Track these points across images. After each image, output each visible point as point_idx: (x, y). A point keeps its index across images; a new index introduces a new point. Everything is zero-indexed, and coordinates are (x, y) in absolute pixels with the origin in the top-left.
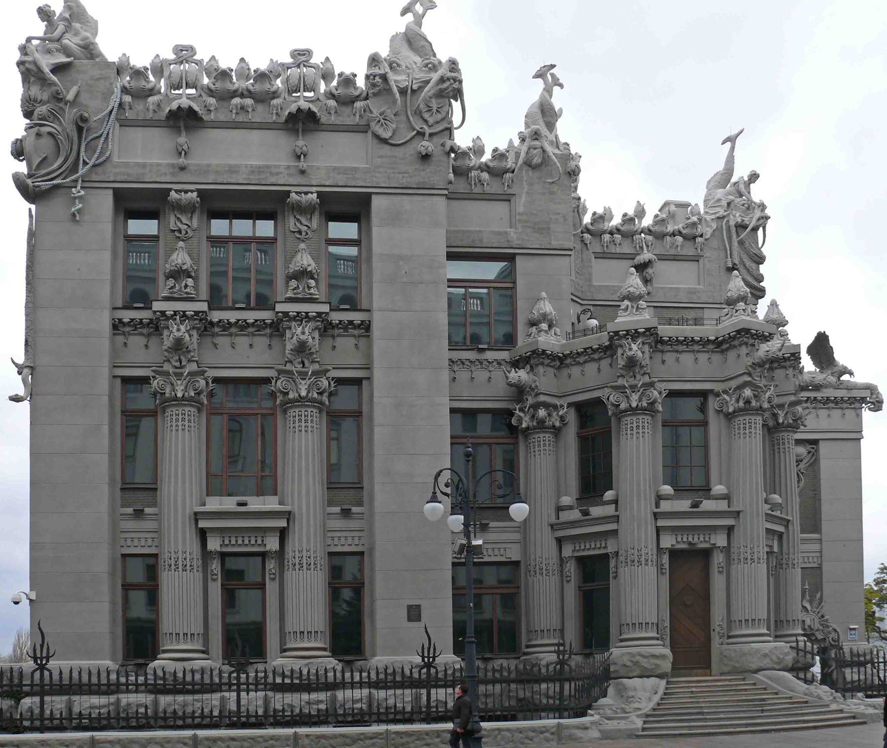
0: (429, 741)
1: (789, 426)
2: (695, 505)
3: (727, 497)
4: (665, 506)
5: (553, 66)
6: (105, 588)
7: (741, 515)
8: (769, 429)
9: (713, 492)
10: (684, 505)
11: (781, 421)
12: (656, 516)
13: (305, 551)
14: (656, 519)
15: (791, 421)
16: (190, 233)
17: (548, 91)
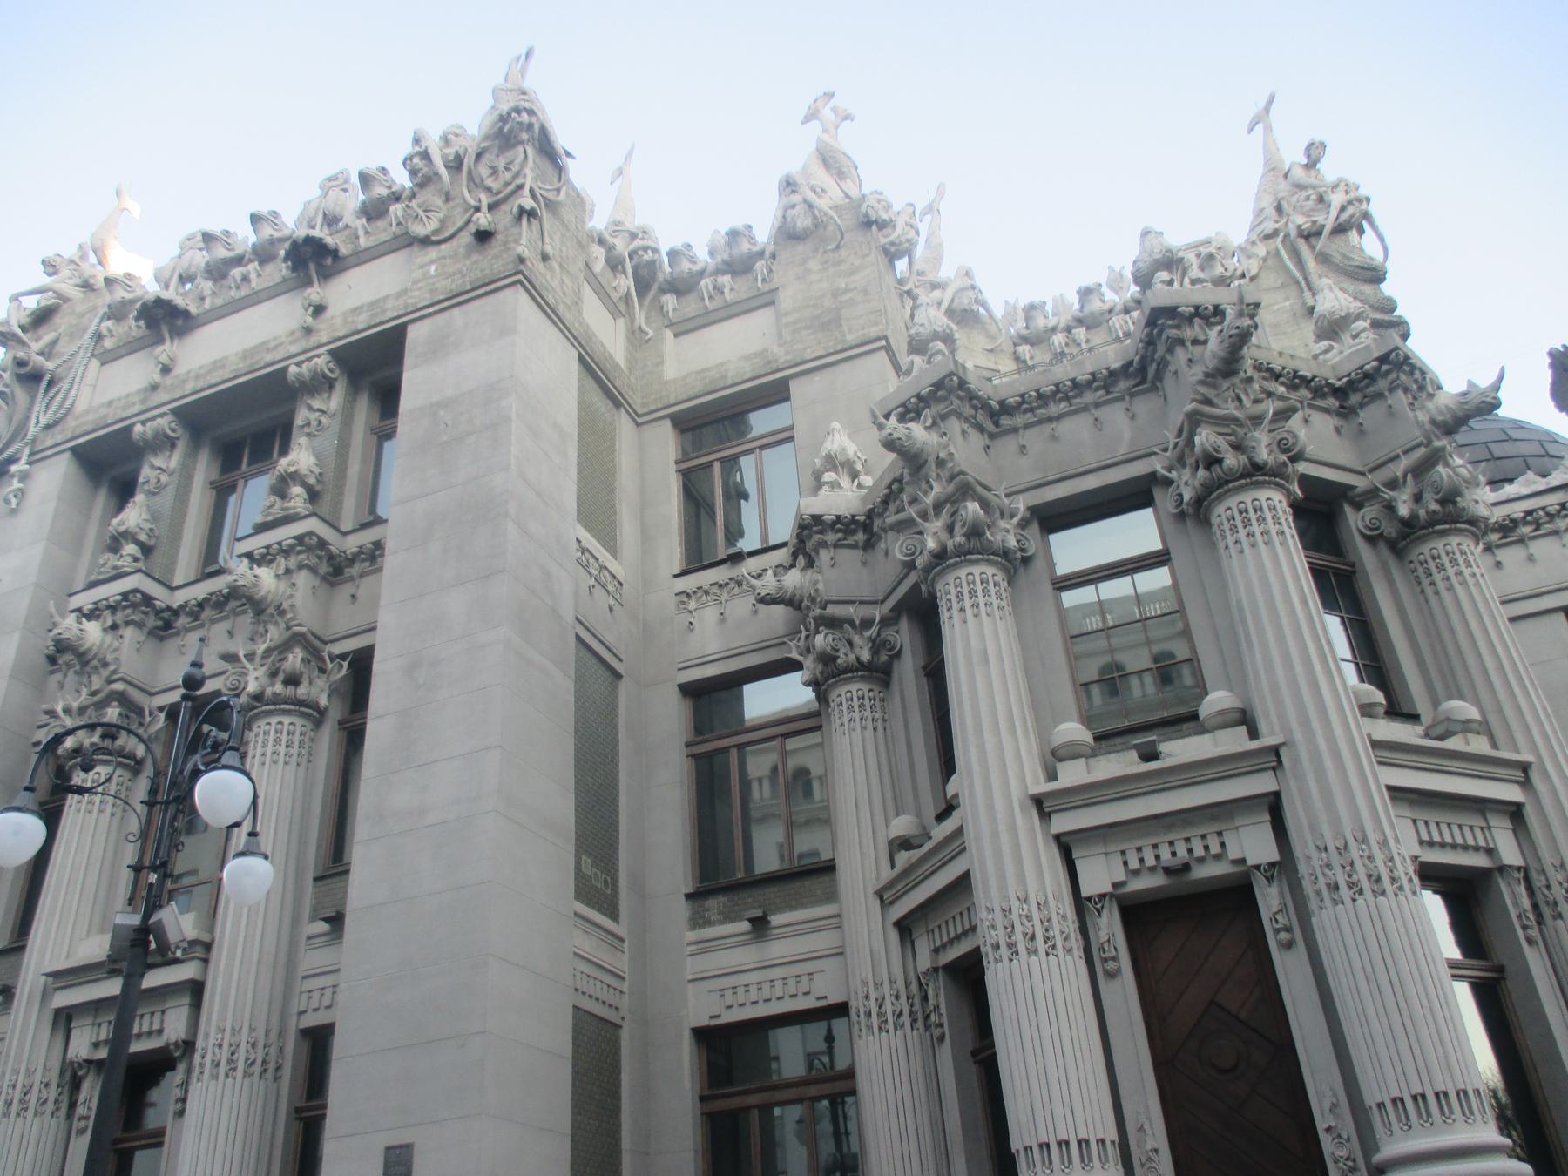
2: (1149, 755)
4: (1072, 774)
7: (1283, 752)
10: (1120, 763)
11: (1404, 511)
12: (1042, 805)
13: (245, 1030)
14: (1045, 816)
15: (1434, 506)
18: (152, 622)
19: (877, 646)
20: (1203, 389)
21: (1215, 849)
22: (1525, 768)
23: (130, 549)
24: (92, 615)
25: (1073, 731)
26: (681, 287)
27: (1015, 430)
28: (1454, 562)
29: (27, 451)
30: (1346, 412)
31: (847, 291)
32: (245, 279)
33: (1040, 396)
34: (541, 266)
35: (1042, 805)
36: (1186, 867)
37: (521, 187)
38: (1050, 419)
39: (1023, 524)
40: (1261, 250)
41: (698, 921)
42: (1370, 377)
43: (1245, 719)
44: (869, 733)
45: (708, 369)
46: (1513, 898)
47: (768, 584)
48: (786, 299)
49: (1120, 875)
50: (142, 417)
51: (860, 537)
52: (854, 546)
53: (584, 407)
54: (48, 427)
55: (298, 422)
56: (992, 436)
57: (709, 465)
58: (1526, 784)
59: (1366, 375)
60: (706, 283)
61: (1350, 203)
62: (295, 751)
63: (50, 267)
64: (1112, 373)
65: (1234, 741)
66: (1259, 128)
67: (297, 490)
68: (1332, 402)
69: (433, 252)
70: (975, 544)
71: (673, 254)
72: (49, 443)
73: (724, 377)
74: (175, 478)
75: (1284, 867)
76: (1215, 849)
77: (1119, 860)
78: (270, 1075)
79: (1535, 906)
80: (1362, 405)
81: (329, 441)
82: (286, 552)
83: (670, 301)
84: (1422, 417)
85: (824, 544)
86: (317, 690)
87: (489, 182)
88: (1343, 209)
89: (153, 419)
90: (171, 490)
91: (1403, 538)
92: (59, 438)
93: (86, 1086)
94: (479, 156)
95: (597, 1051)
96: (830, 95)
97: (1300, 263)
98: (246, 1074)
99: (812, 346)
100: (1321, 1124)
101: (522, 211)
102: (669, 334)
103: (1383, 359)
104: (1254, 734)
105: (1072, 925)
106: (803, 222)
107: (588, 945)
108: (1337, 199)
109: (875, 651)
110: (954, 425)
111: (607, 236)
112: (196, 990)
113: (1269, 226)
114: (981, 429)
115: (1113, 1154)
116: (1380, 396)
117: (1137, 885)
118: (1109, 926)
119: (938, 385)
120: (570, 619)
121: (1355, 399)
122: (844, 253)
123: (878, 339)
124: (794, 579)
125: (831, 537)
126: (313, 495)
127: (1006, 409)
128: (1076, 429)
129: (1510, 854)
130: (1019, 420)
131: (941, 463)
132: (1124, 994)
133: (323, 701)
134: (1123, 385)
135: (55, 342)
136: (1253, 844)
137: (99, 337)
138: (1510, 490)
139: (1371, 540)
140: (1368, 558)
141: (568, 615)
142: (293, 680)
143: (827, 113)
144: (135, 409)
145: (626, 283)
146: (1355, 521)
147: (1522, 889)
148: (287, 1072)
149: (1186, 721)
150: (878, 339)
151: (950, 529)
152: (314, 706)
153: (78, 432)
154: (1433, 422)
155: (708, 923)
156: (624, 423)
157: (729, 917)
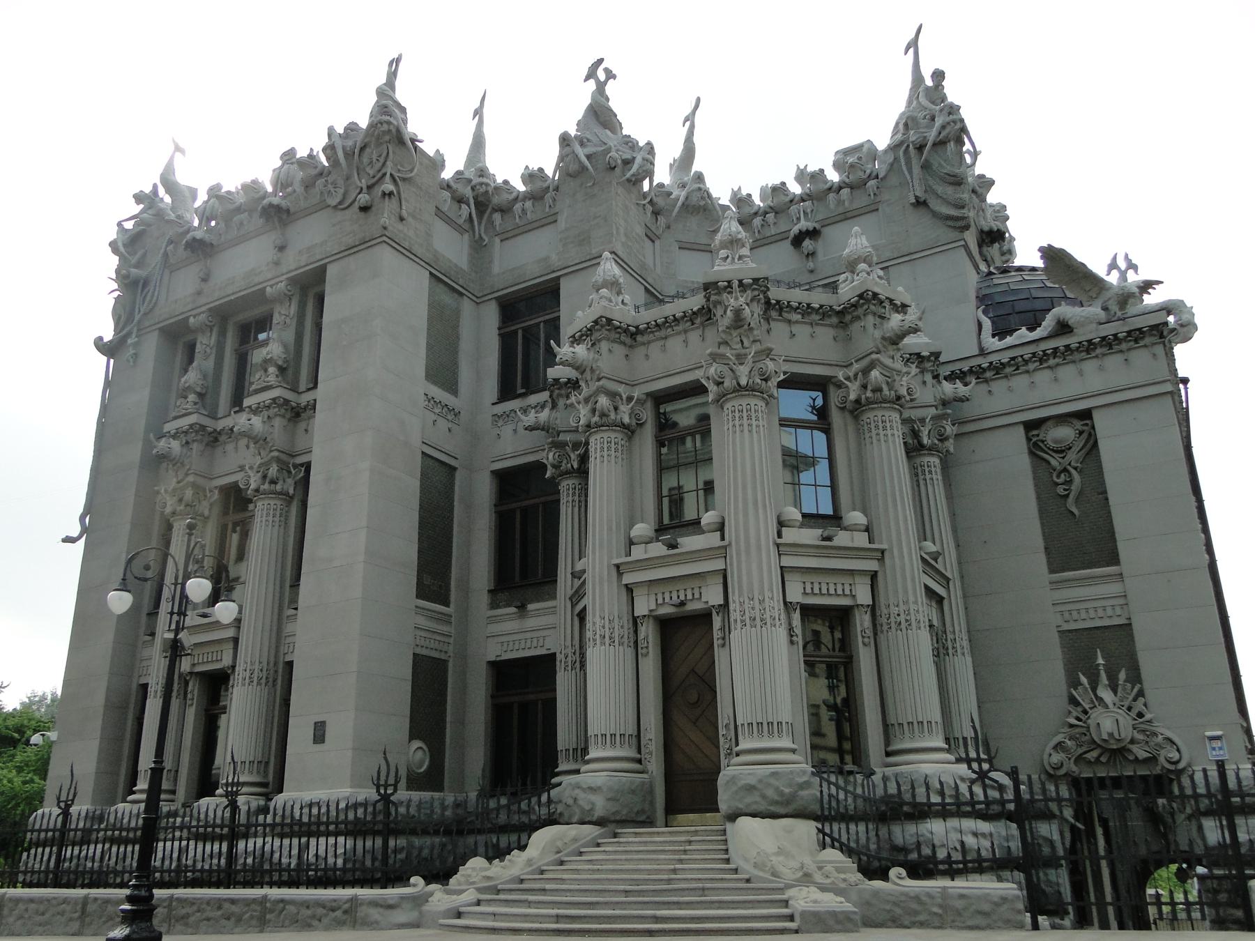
0: (211, 914)
1: (869, 402)
2: (672, 546)
4: (638, 553)
6: (98, 723)
8: (851, 412)
9: (703, 522)
10: (658, 549)
14: (620, 574)
15: (869, 394)
18: (206, 439)
20: (724, 336)
21: (697, 596)
22: (883, 552)
24: (174, 437)
25: (642, 529)
27: (644, 344)
28: (877, 427)
29: (135, 330)
30: (843, 325)
31: (595, 218)
32: (241, 224)
33: (657, 325)
34: (400, 226)
36: (682, 604)
37: (385, 174)
41: (494, 605)
42: (855, 306)
43: (721, 527)
44: (576, 509)
46: (862, 621)
47: (530, 419)
49: (653, 607)
50: (193, 313)
54: (145, 314)
55: (275, 321)
57: (515, 332)
58: (881, 560)
59: (853, 305)
60: (518, 206)
62: (277, 519)
63: (139, 198)
64: (694, 313)
65: (713, 540)
66: (911, 51)
67: (272, 370)
68: (835, 320)
69: (340, 215)
70: (603, 422)
72: (147, 324)
74: (214, 351)
75: (725, 606)
76: (697, 596)
77: (653, 598)
78: (270, 683)
79: (874, 625)
80: (852, 322)
81: (290, 336)
83: (497, 217)
84: (878, 334)
86: (289, 486)
87: (368, 169)
88: (943, 127)
90: (213, 356)
91: (856, 409)
93: (191, 684)
94: (362, 149)
95: (429, 678)
96: (600, 61)
98: (259, 683)
100: (721, 733)
101: (384, 194)
102: (497, 240)
103: (861, 296)
104: (723, 538)
106: (573, 167)
107: (423, 622)
108: (939, 122)
110: (604, 346)
111: (452, 184)
112: (236, 641)
114: (624, 344)
115: (634, 740)
116: (858, 318)
117: (664, 611)
118: (648, 632)
121: (848, 318)
124: (544, 415)
127: (638, 331)
128: (675, 344)
130: (645, 338)
131: (592, 370)
132: (651, 667)
133: (291, 492)
135: (145, 255)
136: (713, 596)
137: (166, 255)
138: (1009, 340)
139: (843, 409)
140: (836, 418)
141: (416, 442)
142: (273, 482)
143: (601, 75)
144: (189, 307)
146: (835, 396)
148: (279, 681)
152: (287, 494)
154: (883, 338)
155: (498, 607)
156: (467, 306)
157: (508, 605)
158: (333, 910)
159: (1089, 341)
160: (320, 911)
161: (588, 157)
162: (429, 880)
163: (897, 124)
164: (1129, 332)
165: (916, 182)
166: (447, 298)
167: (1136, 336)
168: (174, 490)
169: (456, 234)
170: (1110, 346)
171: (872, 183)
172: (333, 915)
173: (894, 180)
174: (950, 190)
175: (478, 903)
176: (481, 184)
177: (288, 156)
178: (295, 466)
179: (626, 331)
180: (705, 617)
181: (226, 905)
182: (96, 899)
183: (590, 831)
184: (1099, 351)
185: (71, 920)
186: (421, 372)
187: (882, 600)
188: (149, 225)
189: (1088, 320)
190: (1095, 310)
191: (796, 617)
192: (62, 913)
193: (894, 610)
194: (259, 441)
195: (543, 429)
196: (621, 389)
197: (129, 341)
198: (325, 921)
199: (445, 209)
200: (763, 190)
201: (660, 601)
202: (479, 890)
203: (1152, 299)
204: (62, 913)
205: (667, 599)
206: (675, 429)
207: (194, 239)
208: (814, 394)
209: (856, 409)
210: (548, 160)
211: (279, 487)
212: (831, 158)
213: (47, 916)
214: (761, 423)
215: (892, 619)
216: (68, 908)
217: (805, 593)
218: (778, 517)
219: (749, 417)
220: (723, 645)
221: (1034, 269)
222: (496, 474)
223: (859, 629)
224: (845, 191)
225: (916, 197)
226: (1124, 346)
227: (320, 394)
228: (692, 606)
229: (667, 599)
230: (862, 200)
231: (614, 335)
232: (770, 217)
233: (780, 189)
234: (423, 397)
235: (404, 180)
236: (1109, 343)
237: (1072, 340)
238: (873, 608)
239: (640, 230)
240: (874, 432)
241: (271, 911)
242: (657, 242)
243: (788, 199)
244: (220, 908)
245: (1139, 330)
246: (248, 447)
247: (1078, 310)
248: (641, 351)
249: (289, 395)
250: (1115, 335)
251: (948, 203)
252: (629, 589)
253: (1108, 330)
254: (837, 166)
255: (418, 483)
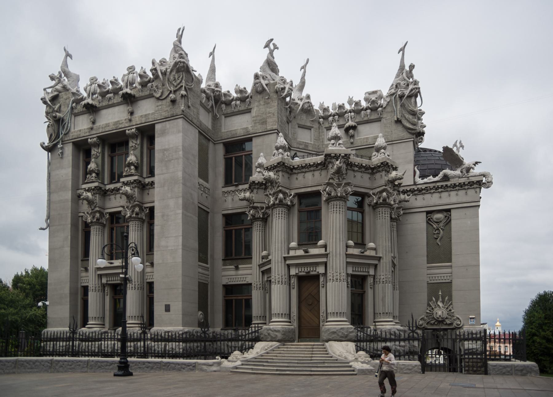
2: (306, 252)
3: (325, 246)
4: (292, 253)
5: (272, 40)
10: (300, 252)
16: (98, 154)
17: (271, 53)
19: (264, 214)
21: (314, 269)
22: (380, 258)
23: (94, 175)
25: (294, 244)
26: (228, 104)
27: (295, 173)
31: (269, 113)
33: (302, 167)
35: (285, 259)
36: (309, 272)
38: (303, 172)
39: (294, 197)
40: (388, 100)
45: (233, 131)
46: (370, 280)
47: (242, 195)
48: (254, 112)
49: (297, 272)
51: (264, 187)
52: (262, 189)
53: (200, 145)
56: (291, 174)
58: (379, 260)
60: (234, 103)
61: (414, 89)
70: (281, 204)
71: (225, 95)
72: (66, 139)
73: (236, 134)
75: (325, 274)
76: (314, 269)
77: (297, 269)
81: (138, 152)
82: (132, 183)
85: (255, 188)
89: (93, 138)
92: (68, 138)
97: (396, 106)
99: (259, 128)
105: (287, 280)
109: (263, 215)
110: (280, 173)
113: (393, 91)
114: (288, 173)
117: (300, 274)
118: (294, 281)
119: (278, 163)
120: (196, 203)
122: (270, 100)
123: (275, 130)
124: (248, 194)
125: (256, 187)
126: (136, 168)
128: (309, 175)
129: (372, 272)
130: (296, 171)
131: (276, 183)
132: (294, 293)
134: (319, 167)
140: (367, 208)
145: (212, 103)
147: (372, 279)
149: (315, 245)
150: (275, 130)
151: (276, 199)
153: (73, 137)
158: (189, 366)
159: (455, 184)
160: (184, 366)
161: (267, 85)
162: (222, 358)
163: (392, 85)
164: (469, 183)
165: (398, 112)
166: (204, 141)
167: (471, 184)
168: (91, 213)
169: (207, 113)
170: (461, 187)
171: (380, 109)
172: (189, 367)
173: (389, 109)
174: (411, 117)
175: (242, 365)
176: (217, 91)
177: (131, 69)
178: (145, 208)
179: (289, 168)
180: (317, 277)
181: (146, 364)
182: (93, 361)
183: (276, 344)
184: (457, 188)
185: (84, 367)
186: (197, 173)
187: (378, 274)
188: (60, 92)
189: (454, 177)
190: (458, 172)
191: (349, 278)
192: (79, 365)
193: (382, 277)
194: (129, 197)
195: (247, 200)
196: (287, 191)
197: (59, 146)
198: (186, 369)
199: (203, 102)
200: (334, 104)
201: (300, 270)
202: (242, 361)
203: (477, 170)
204: (79, 365)
205: (303, 270)
206: (309, 208)
207: (88, 104)
208: (357, 198)
209: (375, 207)
210: (249, 86)
211: (139, 216)
212: (364, 96)
213: (73, 366)
214: (341, 210)
215: (381, 280)
216: (81, 364)
217: (353, 271)
218: (346, 244)
219: (336, 208)
220: (323, 287)
221: (440, 152)
222: (224, 215)
223: (369, 282)
224: (369, 111)
225: (398, 119)
226: (466, 187)
227: (156, 179)
228: (312, 273)
229: (303, 270)
230: (374, 116)
231: (285, 169)
232: (336, 117)
233: (341, 107)
234: (197, 184)
235: (189, 89)
236: (462, 186)
237: (449, 183)
238: (374, 277)
239: (285, 119)
240: (381, 215)
241: (164, 366)
242: (290, 124)
243: (344, 111)
244: (144, 364)
245: (473, 182)
246: (121, 198)
247: (452, 172)
248: (295, 176)
249: (141, 179)
250: (464, 183)
251: (410, 122)
252: (289, 266)
253: (462, 180)
254: (366, 100)
255: (197, 218)
